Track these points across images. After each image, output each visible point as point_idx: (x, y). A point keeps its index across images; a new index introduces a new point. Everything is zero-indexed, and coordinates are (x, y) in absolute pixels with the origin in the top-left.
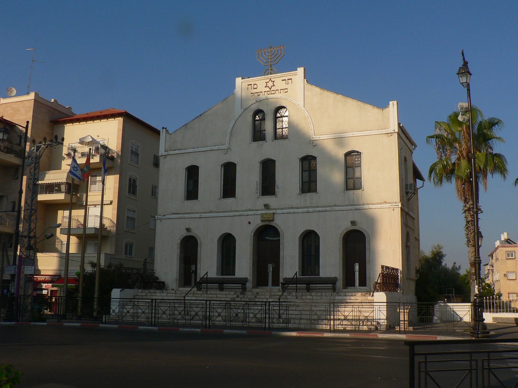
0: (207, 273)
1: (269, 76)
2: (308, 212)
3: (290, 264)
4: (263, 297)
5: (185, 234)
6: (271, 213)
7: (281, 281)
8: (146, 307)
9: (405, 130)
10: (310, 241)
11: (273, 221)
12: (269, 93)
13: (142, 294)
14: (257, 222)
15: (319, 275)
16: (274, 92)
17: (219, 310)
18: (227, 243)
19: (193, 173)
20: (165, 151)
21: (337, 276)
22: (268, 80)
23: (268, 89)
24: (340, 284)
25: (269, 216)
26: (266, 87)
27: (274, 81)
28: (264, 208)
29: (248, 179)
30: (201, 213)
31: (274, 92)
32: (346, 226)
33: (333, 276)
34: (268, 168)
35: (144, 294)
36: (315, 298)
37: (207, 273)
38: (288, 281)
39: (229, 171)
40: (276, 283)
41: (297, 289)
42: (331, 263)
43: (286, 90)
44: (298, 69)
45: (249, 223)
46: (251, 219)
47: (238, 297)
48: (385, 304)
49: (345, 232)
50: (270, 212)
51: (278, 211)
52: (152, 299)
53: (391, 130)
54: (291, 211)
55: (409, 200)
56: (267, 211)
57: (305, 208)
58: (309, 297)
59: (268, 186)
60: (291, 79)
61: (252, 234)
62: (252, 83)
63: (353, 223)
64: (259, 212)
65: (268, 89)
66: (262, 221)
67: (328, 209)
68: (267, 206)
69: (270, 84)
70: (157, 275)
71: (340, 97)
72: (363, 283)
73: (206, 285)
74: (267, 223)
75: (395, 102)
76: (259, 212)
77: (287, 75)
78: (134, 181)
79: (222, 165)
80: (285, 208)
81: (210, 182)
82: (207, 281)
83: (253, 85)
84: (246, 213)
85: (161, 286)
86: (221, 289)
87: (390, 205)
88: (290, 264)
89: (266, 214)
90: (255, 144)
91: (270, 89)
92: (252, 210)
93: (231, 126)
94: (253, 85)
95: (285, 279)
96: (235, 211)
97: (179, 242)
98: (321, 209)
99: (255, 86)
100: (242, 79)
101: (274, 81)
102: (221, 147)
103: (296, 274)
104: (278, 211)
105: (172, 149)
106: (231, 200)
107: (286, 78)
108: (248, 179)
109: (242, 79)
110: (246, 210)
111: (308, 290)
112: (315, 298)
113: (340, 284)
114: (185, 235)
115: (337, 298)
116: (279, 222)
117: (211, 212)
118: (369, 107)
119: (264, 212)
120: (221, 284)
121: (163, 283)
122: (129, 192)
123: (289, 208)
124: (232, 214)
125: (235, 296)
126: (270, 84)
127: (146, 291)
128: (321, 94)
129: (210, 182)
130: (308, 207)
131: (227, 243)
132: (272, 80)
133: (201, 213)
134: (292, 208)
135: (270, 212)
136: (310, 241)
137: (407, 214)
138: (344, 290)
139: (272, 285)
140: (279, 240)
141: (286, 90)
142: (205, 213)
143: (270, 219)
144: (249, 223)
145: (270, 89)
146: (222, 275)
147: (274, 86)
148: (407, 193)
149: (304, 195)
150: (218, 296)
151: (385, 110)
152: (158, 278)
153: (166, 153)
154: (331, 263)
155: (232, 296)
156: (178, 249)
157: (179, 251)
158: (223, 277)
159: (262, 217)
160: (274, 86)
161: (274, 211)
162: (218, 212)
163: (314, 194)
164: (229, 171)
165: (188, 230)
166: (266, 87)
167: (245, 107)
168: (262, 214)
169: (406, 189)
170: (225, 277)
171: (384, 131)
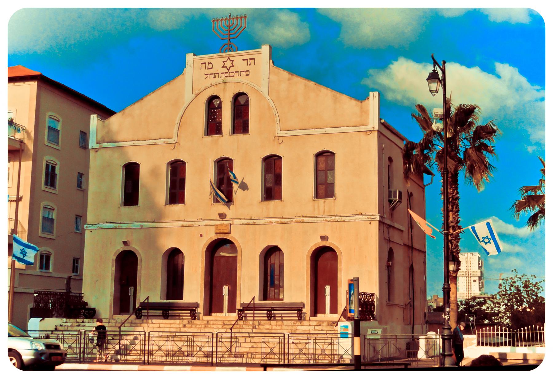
0: (148, 298)
1: (227, 53)
2: (271, 223)
4: (215, 326)
5: (120, 248)
6: (227, 225)
7: (238, 307)
8: (73, 341)
9: (389, 126)
12: (226, 75)
13: (67, 324)
14: (211, 236)
16: (232, 74)
17: (161, 343)
20: (97, 143)
22: (226, 59)
23: (225, 70)
24: (307, 310)
25: (224, 228)
26: (223, 67)
27: (233, 61)
28: (218, 218)
30: (142, 222)
31: (232, 74)
32: (316, 242)
33: (299, 301)
35: (69, 324)
36: (274, 327)
37: (148, 298)
38: (247, 307)
39: (177, 170)
40: (232, 309)
41: (254, 317)
42: (296, 286)
43: (247, 73)
44: (262, 47)
45: (201, 236)
46: (203, 230)
47: (184, 326)
49: (314, 248)
51: (236, 222)
53: (369, 128)
54: (251, 222)
55: (393, 209)
56: (222, 222)
58: (268, 327)
60: (254, 59)
61: (205, 250)
62: (207, 61)
63: (324, 238)
64: (213, 223)
65: (225, 70)
66: (216, 234)
69: (228, 64)
70: (85, 299)
71: (312, 84)
72: (334, 310)
73: (146, 311)
76: (213, 223)
77: (248, 54)
78: (53, 168)
79: (168, 164)
80: (244, 219)
82: (148, 306)
83: (207, 64)
84: (197, 223)
85: (91, 313)
86: (166, 316)
89: (221, 225)
90: (210, 138)
91: (228, 70)
92: (204, 220)
93: (180, 114)
94: (207, 64)
95: (242, 305)
97: (115, 258)
99: (210, 66)
100: (195, 55)
101: (233, 61)
103: (254, 299)
105: (106, 140)
107: (248, 57)
110: (198, 220)
111: (270, 317)
112: (274, 327)
113: (307, 310)
114: (122, 250)
115: (299, 327)
118: (345, 98)
119: (219, 222)
120: (166, 311)
121: (94, 310)
122: (46, 184)
123: (249, 219)
124: (180, 224)
125: (181, 326)
126: (228, 64)
127: (72, 320)
128: (289, 79)
130: (271, 218)
132: (231, 58)
134: (252, 218)
135: (226, 222)
137: (390, 226)
138: (312, 318)
140: (236, 257)
141: (247, 73)
144: (201, 236)
145: (228, 70)
146: (168, 299)
147: (233, 66)
148: (390, 201)
150: (161, 325)
151: (365, 103)
152: (86, 304)
153: (98, 146)
154: (296, 286)
155: (178, 326)
156: (112, 267)
157: (114, 269)
158: (168, 301)
159: (216, 229)
160: (233, 66)
161: (231, 222)
164: (177, 170)
165: (125, 243)
166: (223, 67)
167: (197, 92)
168: (216, 225)
169: (390, 196)
170: (171, 301)
171: (362, 128)
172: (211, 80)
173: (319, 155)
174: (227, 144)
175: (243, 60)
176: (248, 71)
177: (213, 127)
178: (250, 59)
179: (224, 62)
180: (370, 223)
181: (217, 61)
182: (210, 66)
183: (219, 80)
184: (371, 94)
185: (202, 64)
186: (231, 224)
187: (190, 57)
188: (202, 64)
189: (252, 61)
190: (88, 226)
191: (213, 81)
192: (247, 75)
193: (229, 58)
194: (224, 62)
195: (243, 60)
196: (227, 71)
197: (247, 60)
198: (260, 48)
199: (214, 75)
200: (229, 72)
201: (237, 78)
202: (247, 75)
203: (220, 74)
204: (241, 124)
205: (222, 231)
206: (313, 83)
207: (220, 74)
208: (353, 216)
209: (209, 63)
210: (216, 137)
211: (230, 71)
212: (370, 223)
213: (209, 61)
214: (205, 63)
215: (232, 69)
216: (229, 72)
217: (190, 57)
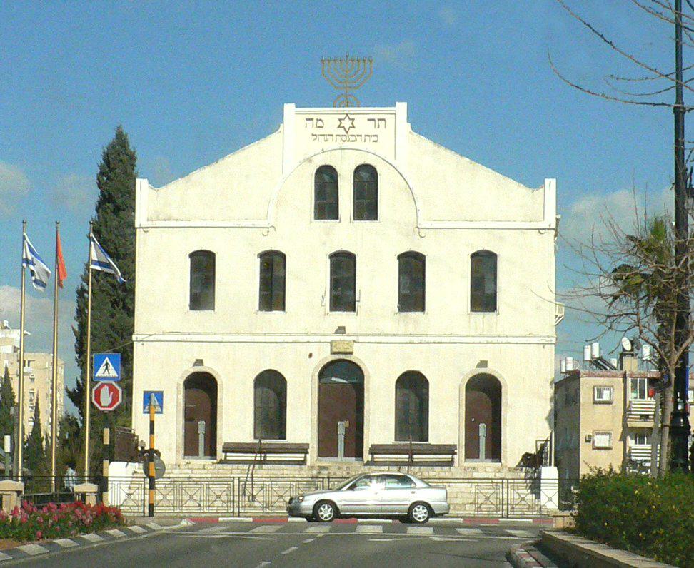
3: (380, 423)
10: (413, 388)
11: (351, 353)
12: (344, 138)
15: (427, 440)
16: (353, 138)
18: (271, 388)
19: (203, 265)
20: (148, 220)
21: (457, 443)
22: (343, 117)
23: (342, 132)
24: (461, 451)
26: (339, 127)
27: (353, 120)
29: (308, 281)
32: (471, 369)
34: (343, 265)
44: (397, 103)
45: (311, 355)
46: (312, 348)
48: (557, 481)
50: (347, 338)
52: (234, 478)
57: (407, 335)
60: (384, 120)
62: (315, 117)
67: (444, 340)
68: (341, 330)
72: (495, 452)
74: (341, 357)
75: (554, 181)
76: (329, 339)
77: (377, 112)
80: (373, 335)
81: (238, 279)
87: (540, 339)
88: (380, 423)
91: (347, 132)
96: (286, 334)
98: (432, 339)
99: (320, 124)
100: (296, 107)
101: (353, 120)
102: (258, 224)
104: (361, 339)
105: (161, 217)
106: (276, 314)
107: (376, 117)
108: (308, 281)
109: (296, 107)
114: (192, 371)
116: (360, 356)
117: (238, 334)
118: (512, 184)
126: (347, 123)
129: (238, 279)
131: (271, 388)
132: (351, 117)
133: (223, 334)
135: (347, 338)
136: (413, 388)
139: (345, 456)
141: (375, 138)
142: (230, 334)
143: (348, 351)
144: (311, 355)
145: (347, 132)
147: (353, 127)
149: (404, 314)
150: (286, 472)
153: (150, 224)
160: (353, 127)
161: (355, 338)
162: (253, 335)
163: (420, 314)
166: (339, 127)
172: (321, 144)
173: (475, 256)
174: (344, 232)
175: (369, 120)
176: (376, 136)
177: (326, 207)
178: (379, 120)
179: (340, 120)
180: (544, 347)
181: (330, 118)
182: (320, 124)
183: (332, 144)
184: (547, 181)
185: (307, 120)
186: (354, 341)
187: (289, 109)
188: (307, 120)
189: (382, 123)
190: (138, 336)
191: (327, 146)
192: (374, 141)
193: (347, 115)
194: (340, 120)
195: (369, 120)
196: (345, 133)
197: (374, 120)
198: (395, 106)
200: (347, 133)
201: (359, 144)
202: (374, 141)
203: (334, 136)
204: (367, 207)
205: (342, 350)
206: (467, 159)
207: (334, 136)
208: (522, 336)
209: (318, 120)
210: (330, 223)
211: (349, 133)
212: (544, 347)
213: (319, 117)
214: (312, 119)
215: (352, 132)
216: (347, 133)
217: (289, 109)
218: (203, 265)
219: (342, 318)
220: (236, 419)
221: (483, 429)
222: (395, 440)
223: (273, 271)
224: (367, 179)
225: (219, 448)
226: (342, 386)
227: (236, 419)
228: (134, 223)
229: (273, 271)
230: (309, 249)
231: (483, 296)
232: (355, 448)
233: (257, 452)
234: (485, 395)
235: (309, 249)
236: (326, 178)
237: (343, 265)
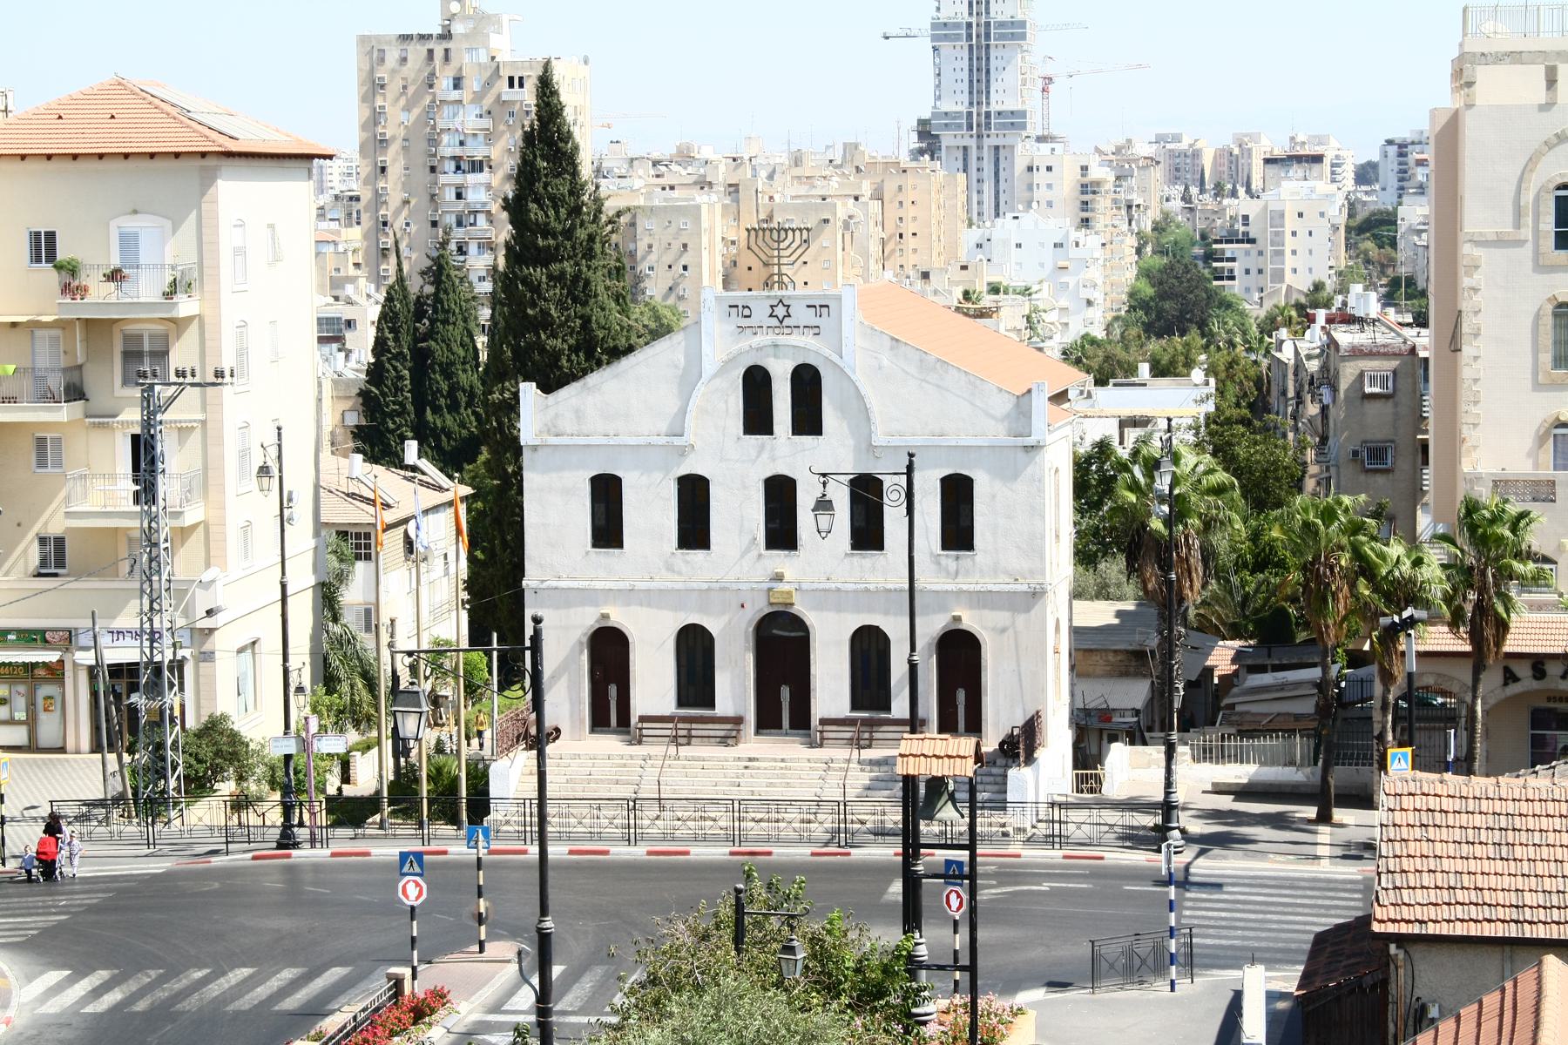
10: (869, 650)
14: (759, 607)
16: (787, 331)
19: (607, 495)
23: (774, 322)
29: (737, 513)
34: (780, 493)
59: (781, 530)
68: (779, 578)
69: (780, 311)
81: (650, 511)
97: (585, 640)
99: (746, 312)
106: (698, 555)
108: (737, 513)
126: (780, 311)
129: (650, 511)
171: (1020, 441)
174: (782, 450)
177: (757, 419)
182: (746, 312)
189: (825, 310)
199: (756, 330)
201: (796, 339)
204: (808, 420)
215: (787, 322)
218: (607, 495)
219: (779, 560)
220: (653, 683)
221: (961, 695)
222: (854, 707)
223: (694, 498)
224: (807, 382)
225: (634, 720)
226: (782, 646)
227: (653, 683)
228: (516, 439)
229: (694, 498)
230: (738, 472)
231: (958, 532)
232: (801, 720)
233: (680, 730)
234: (960, 656)
235: (738, 472)
236: (756, 383)
237: (780, 493)
